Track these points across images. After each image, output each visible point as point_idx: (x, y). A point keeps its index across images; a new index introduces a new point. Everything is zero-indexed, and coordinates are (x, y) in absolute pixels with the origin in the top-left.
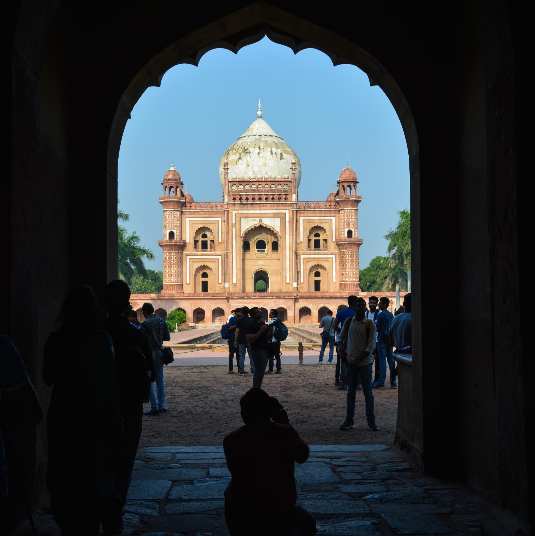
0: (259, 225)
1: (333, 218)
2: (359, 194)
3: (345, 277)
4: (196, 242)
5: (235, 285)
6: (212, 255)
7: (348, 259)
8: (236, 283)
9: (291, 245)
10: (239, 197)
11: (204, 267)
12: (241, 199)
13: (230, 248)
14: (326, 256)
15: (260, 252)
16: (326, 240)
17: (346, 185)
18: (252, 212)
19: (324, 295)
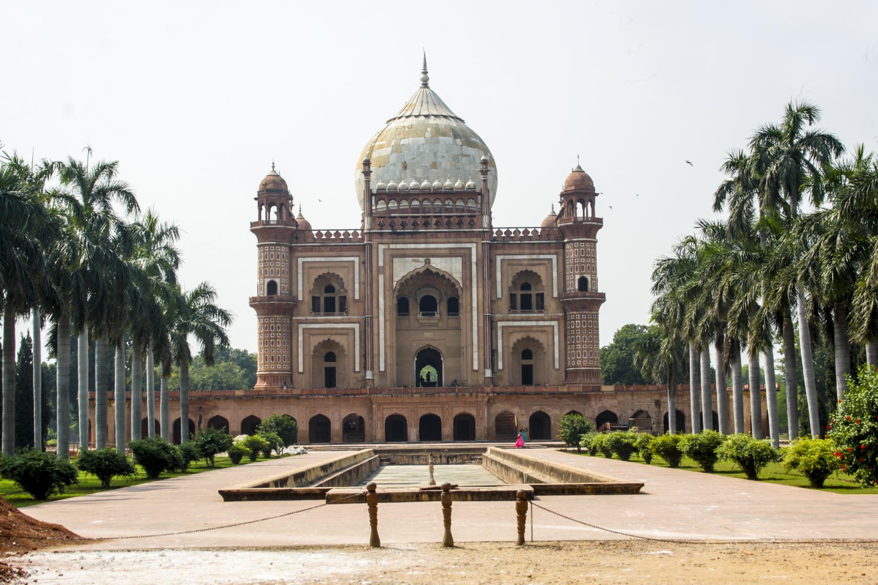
1: (554, 257)
2: (597, 216)
3: (576, 360)
5: (383, 374)
6: (343, 323)
7: (581, 329)
8: (385, 371)
9: (481, 303)
10: (389, 221)
11: (328, 343)
12: (392, 226)
13: (375, 310)
14: (541, 323)
15: (427, 317)
16: (541, 297)
17: (574, 199)
18: (412, 246)
19: (539, 389)
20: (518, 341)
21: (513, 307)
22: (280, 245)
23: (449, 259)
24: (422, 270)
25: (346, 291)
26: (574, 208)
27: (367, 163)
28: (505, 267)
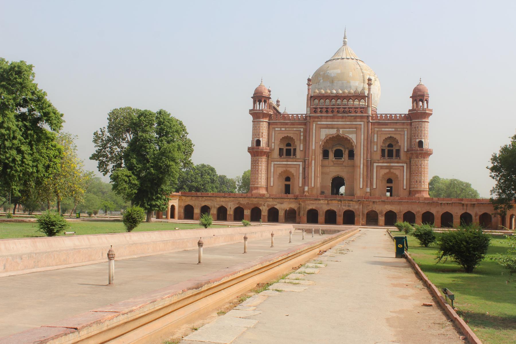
4: (281, 150)
20: (385, 174)
21: (383, 155)
24: (335, 135)
25: (296, 146)
26: (417, 104)
27: (309, 80)
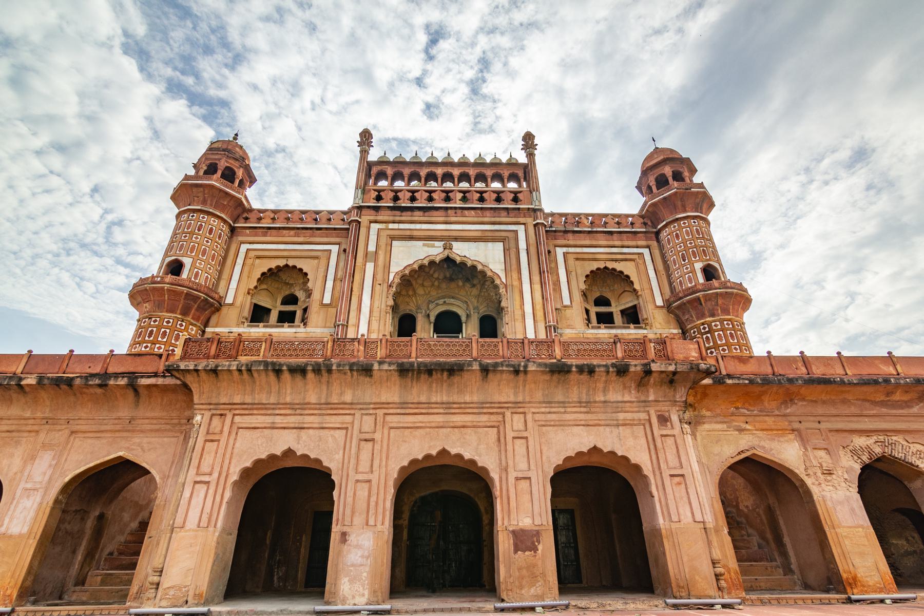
0: (442, 256)
9: (539, 307)
13: (353, 314)
22: (208, 213)
23: (482, 245)
24: (438, 260)
28: (571, 262)
